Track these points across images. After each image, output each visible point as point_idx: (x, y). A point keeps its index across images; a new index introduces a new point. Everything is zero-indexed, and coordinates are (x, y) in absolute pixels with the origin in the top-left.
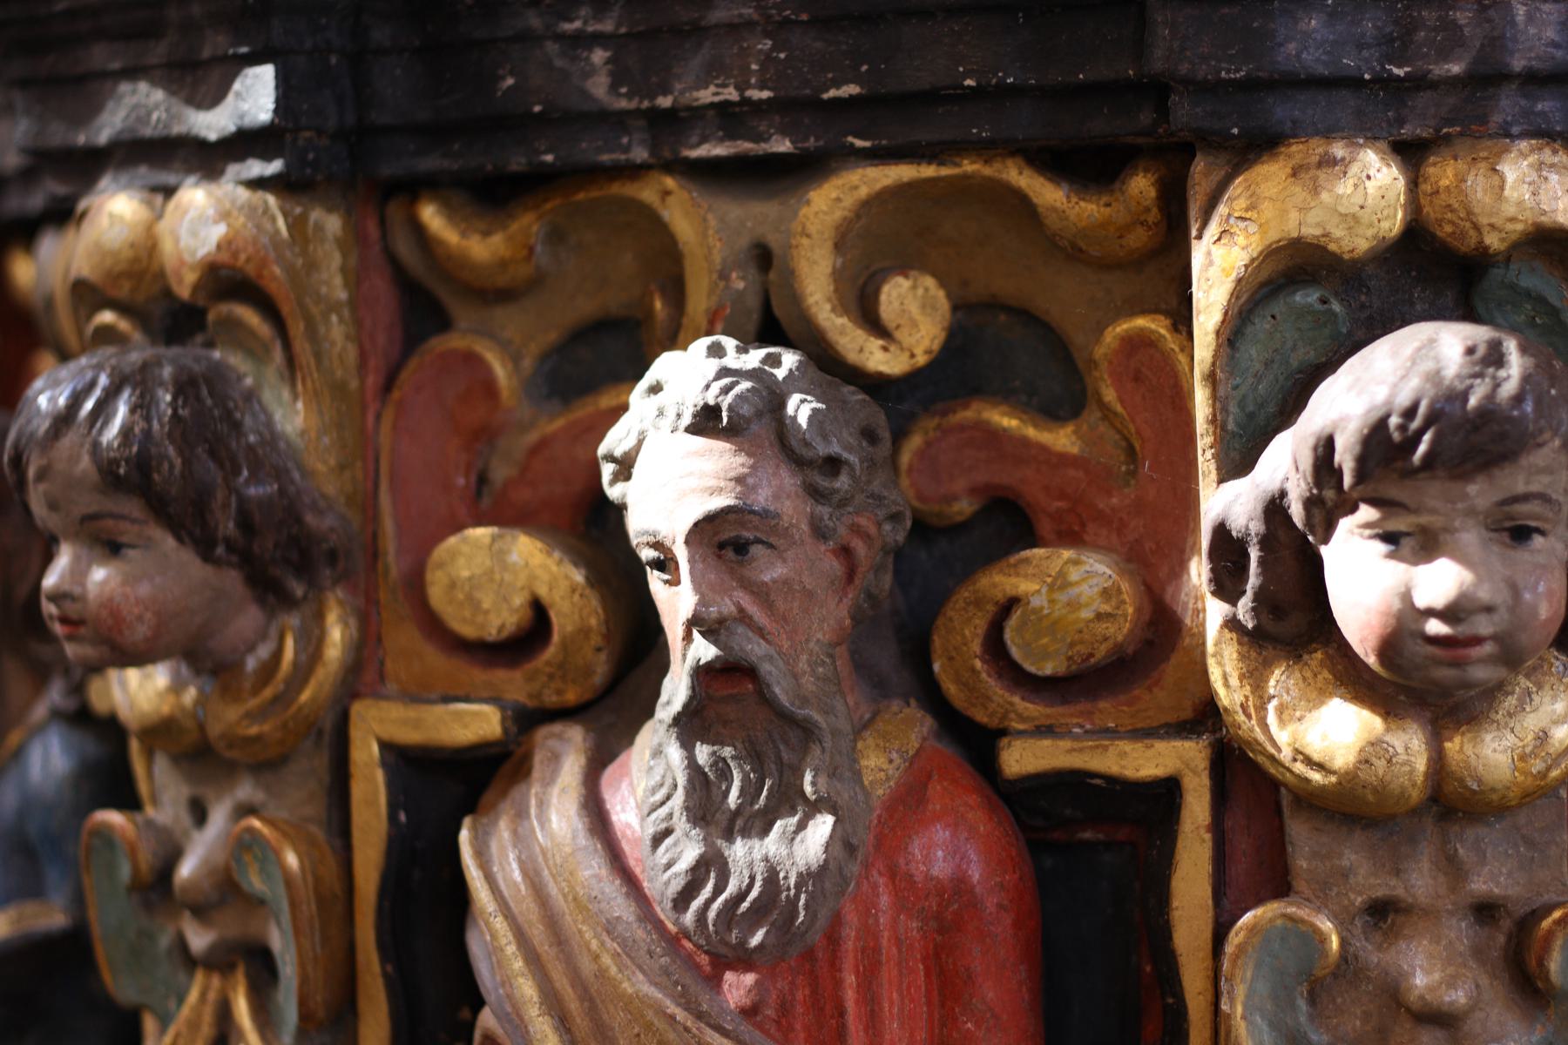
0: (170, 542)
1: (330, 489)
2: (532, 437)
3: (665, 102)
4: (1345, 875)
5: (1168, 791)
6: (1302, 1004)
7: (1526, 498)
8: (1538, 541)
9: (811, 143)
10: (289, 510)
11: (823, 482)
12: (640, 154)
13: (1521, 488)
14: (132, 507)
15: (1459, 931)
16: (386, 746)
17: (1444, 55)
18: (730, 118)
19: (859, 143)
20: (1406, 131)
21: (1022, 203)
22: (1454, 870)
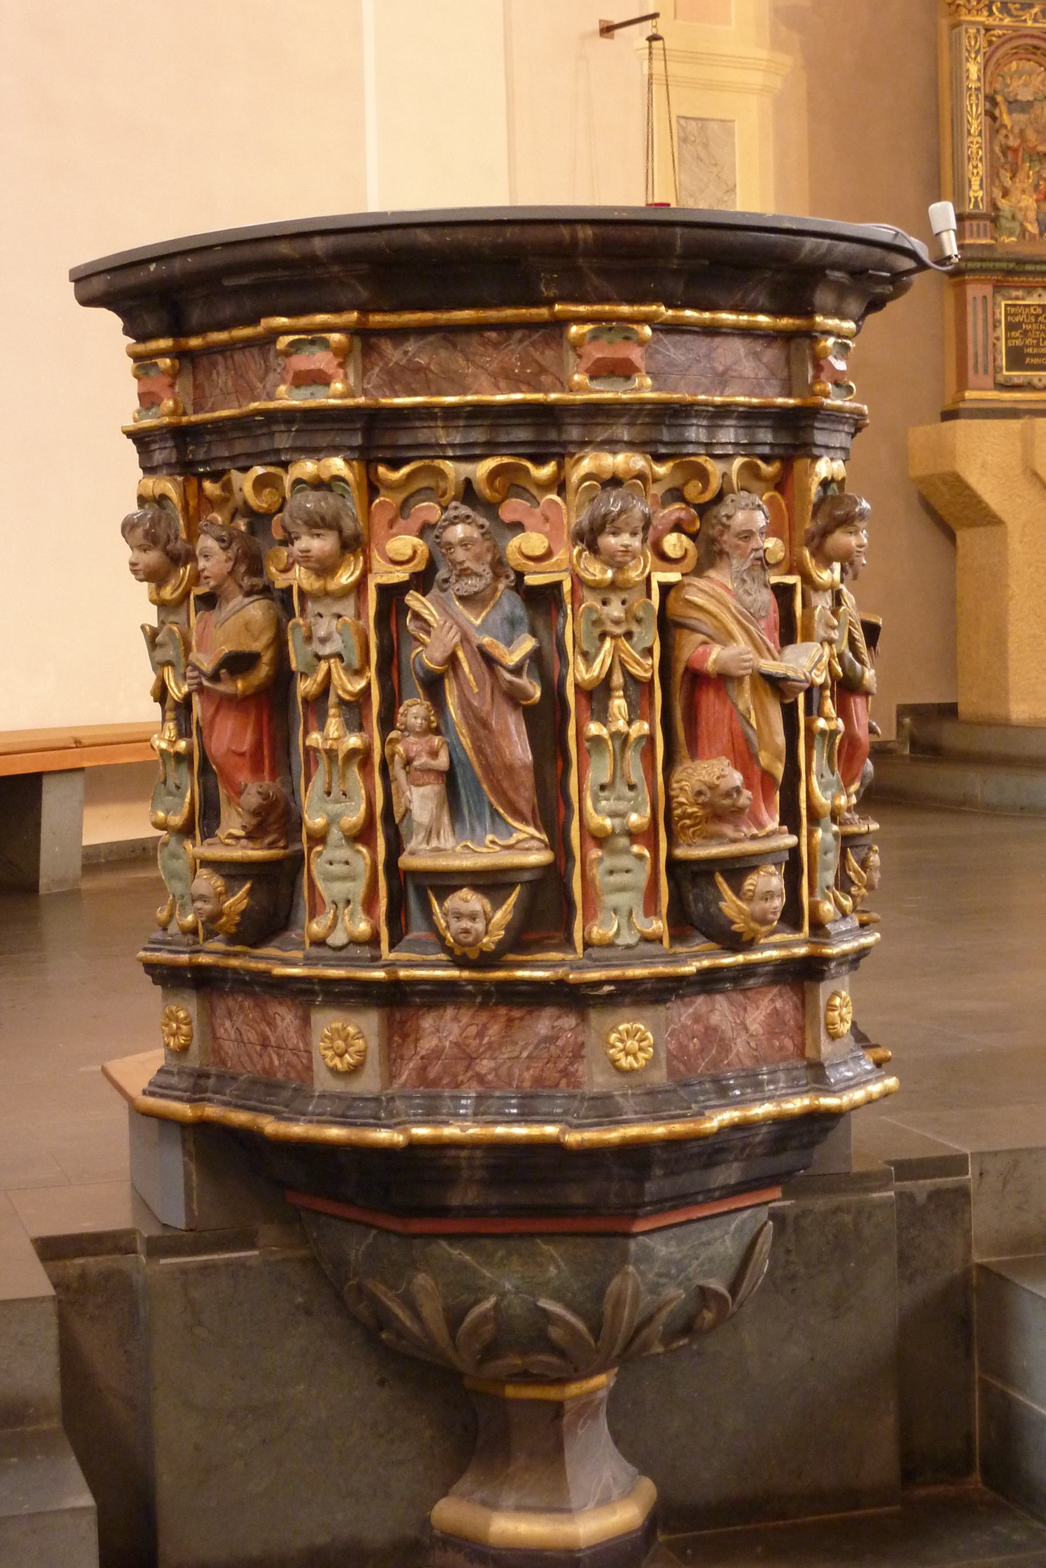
2: (661, 515)
3: (714, 441)
5: (794, 586)
12: (703, 452)
21: (758, 466)
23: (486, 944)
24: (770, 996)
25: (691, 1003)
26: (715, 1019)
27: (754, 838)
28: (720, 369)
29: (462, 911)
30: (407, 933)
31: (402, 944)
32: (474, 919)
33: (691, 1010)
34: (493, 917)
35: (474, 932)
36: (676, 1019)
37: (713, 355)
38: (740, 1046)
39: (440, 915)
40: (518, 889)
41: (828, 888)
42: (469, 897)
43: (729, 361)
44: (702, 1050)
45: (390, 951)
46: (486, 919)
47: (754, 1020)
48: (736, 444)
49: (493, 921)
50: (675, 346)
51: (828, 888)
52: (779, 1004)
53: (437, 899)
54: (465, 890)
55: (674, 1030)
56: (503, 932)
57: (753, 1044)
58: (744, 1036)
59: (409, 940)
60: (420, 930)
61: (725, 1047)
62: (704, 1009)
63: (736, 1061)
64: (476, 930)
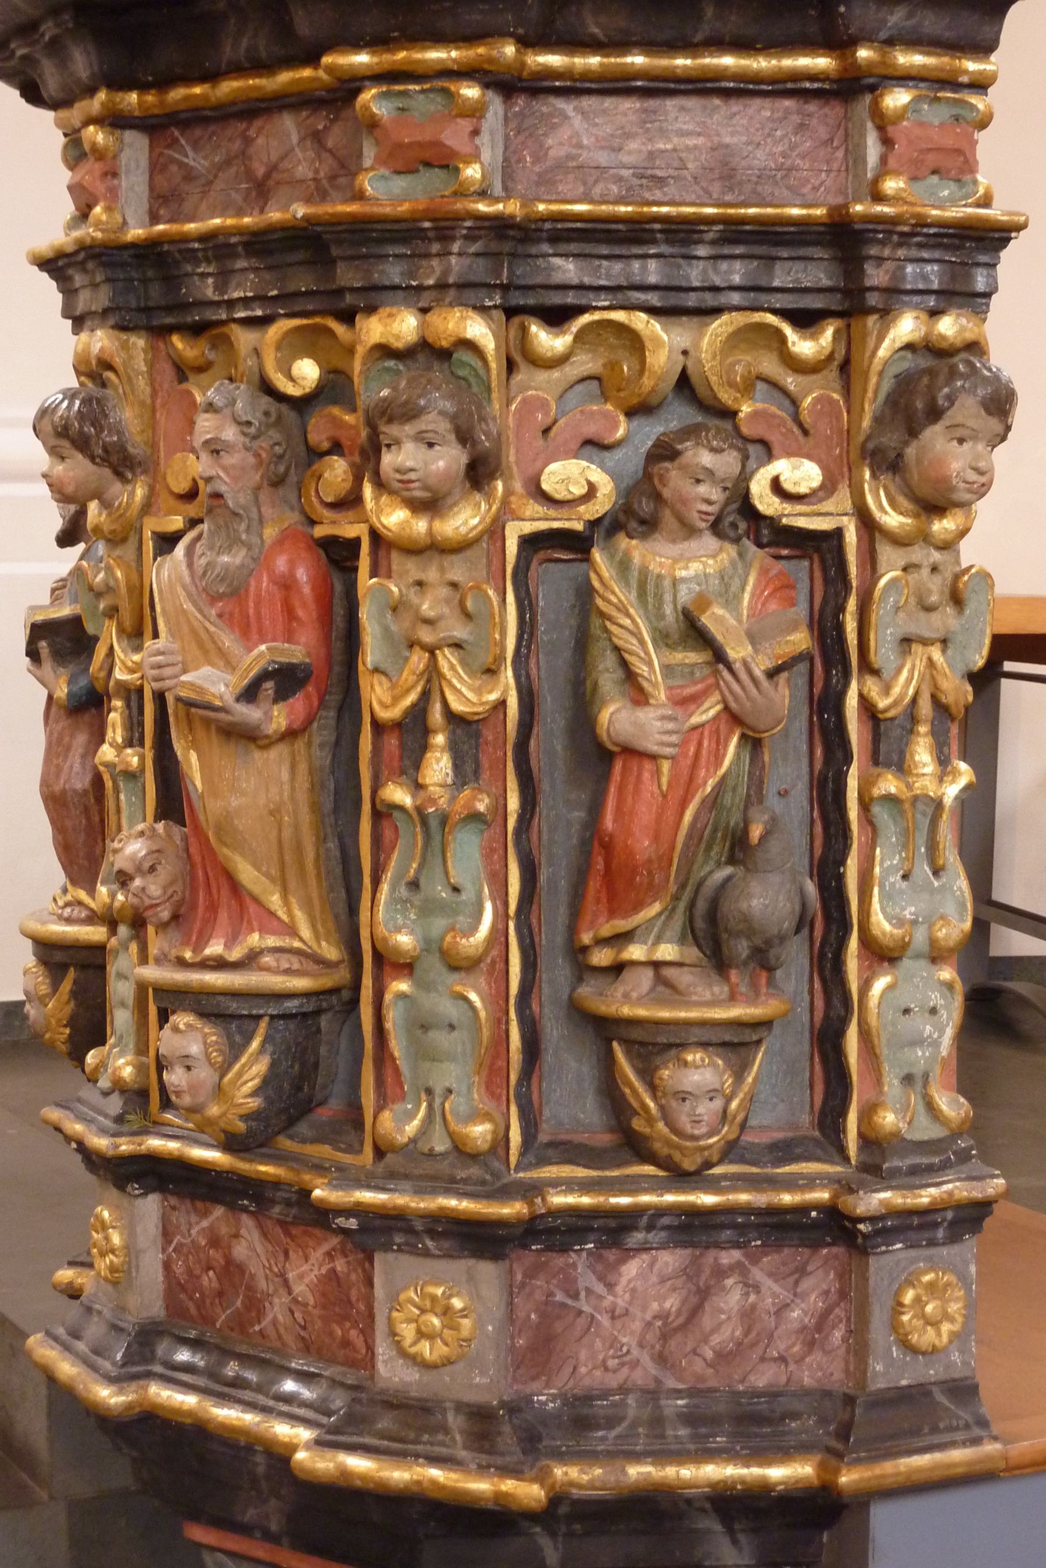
0: (80, 456)
1: (138, 439)
4: (408, 572)
5: (356, 542)
6: (389, 616)
7: (427, 431)
8: (437, 448)
9: (268, 312)
10: (121, 448)
11: (246, 430)
12: (224, 317)
13: (424, 428)
14: (66, 444)
15: (444, 592)
16: (153, 533)
17: (428, 277)
18: (246, 302)
19: (282, 312)
20: (420, 305)
22: (442, 570)
24: (326, 1247)
25: (205, 1214)
26: (240, 1251)
27: (182, 963)
28: (260, 171)
33: (205, 1223)
36: (184, 1228)
37: (252, 150)
38: (277, 1310)
41: (429, 1091)
43: (274, 157)
44: (220, 1294)
47: (301, 1277)
48: (261, 299)
50: (196, 145)
51: (429, 1091)
52: (340, 1265)
55: (181, 1245)
57: (298, 1315)
58: (286, 1299)
61: (256, 1305)
62: (224, 1230)
63: (271, 1332)
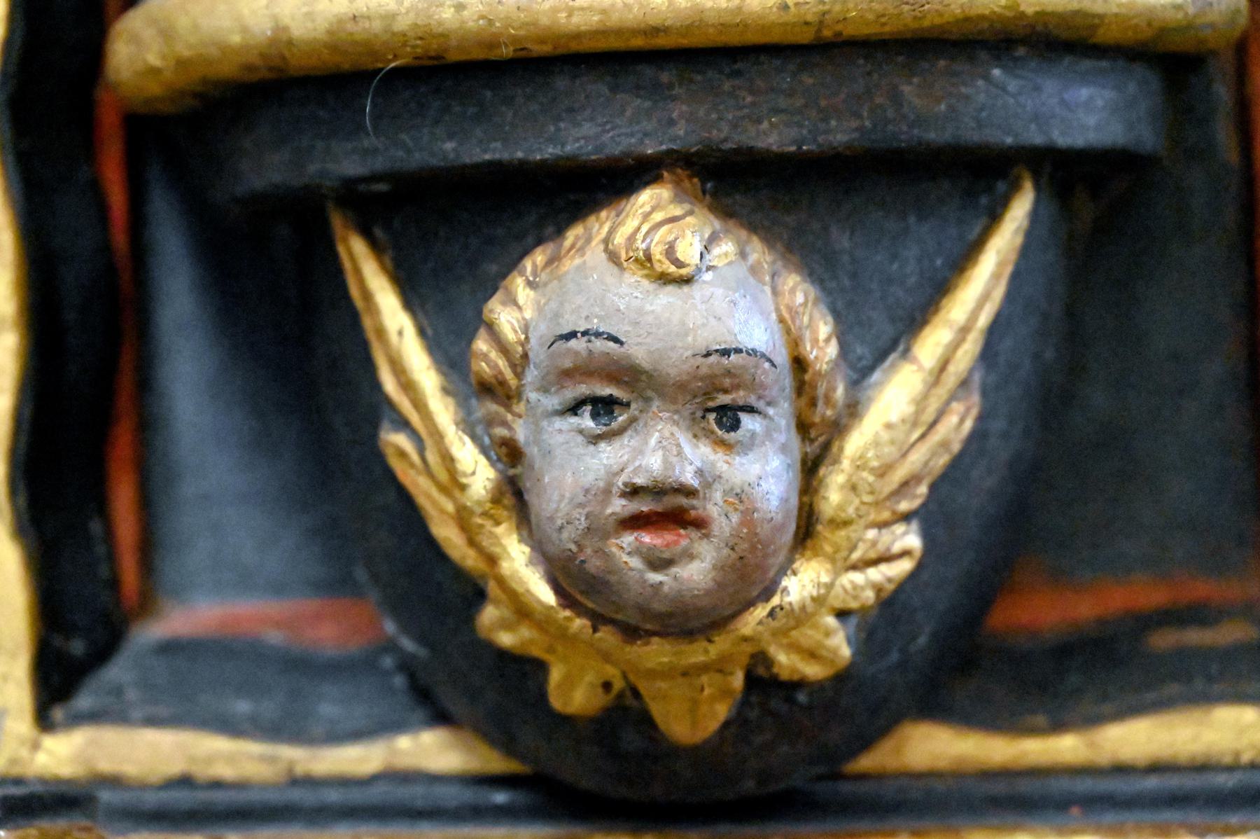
23: (801, 616)
29: (639, 350)
30: (146, 606)
31: (117, 671)
32: (729, 417)
34: (854, 410)
35: (722, 518)
39: (443, 412)
40: (1020, 211)
42: (689, 249)
45: (44, 720)
46: (803, 427)
49: (856, 442)
53: (410, 303)
54: (646, 197)
56: (910, 539)
59: (170, 648)
60: (245, 582)
64: (740, 498)
